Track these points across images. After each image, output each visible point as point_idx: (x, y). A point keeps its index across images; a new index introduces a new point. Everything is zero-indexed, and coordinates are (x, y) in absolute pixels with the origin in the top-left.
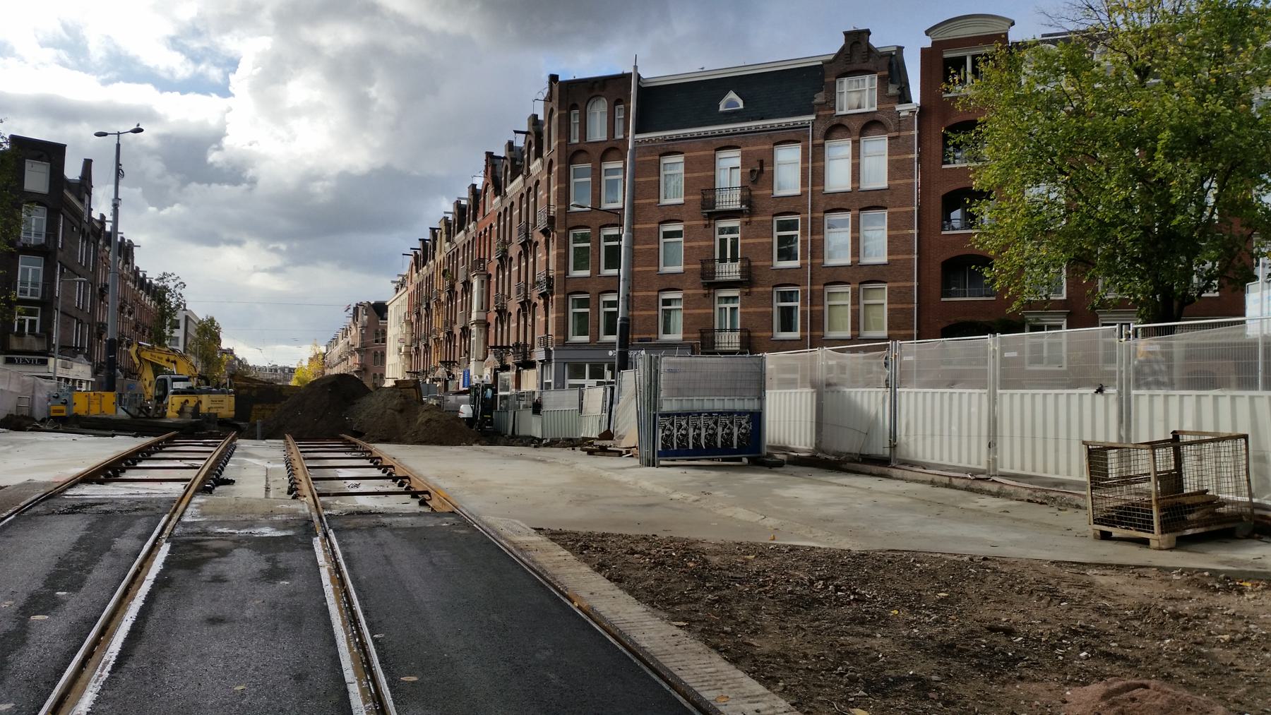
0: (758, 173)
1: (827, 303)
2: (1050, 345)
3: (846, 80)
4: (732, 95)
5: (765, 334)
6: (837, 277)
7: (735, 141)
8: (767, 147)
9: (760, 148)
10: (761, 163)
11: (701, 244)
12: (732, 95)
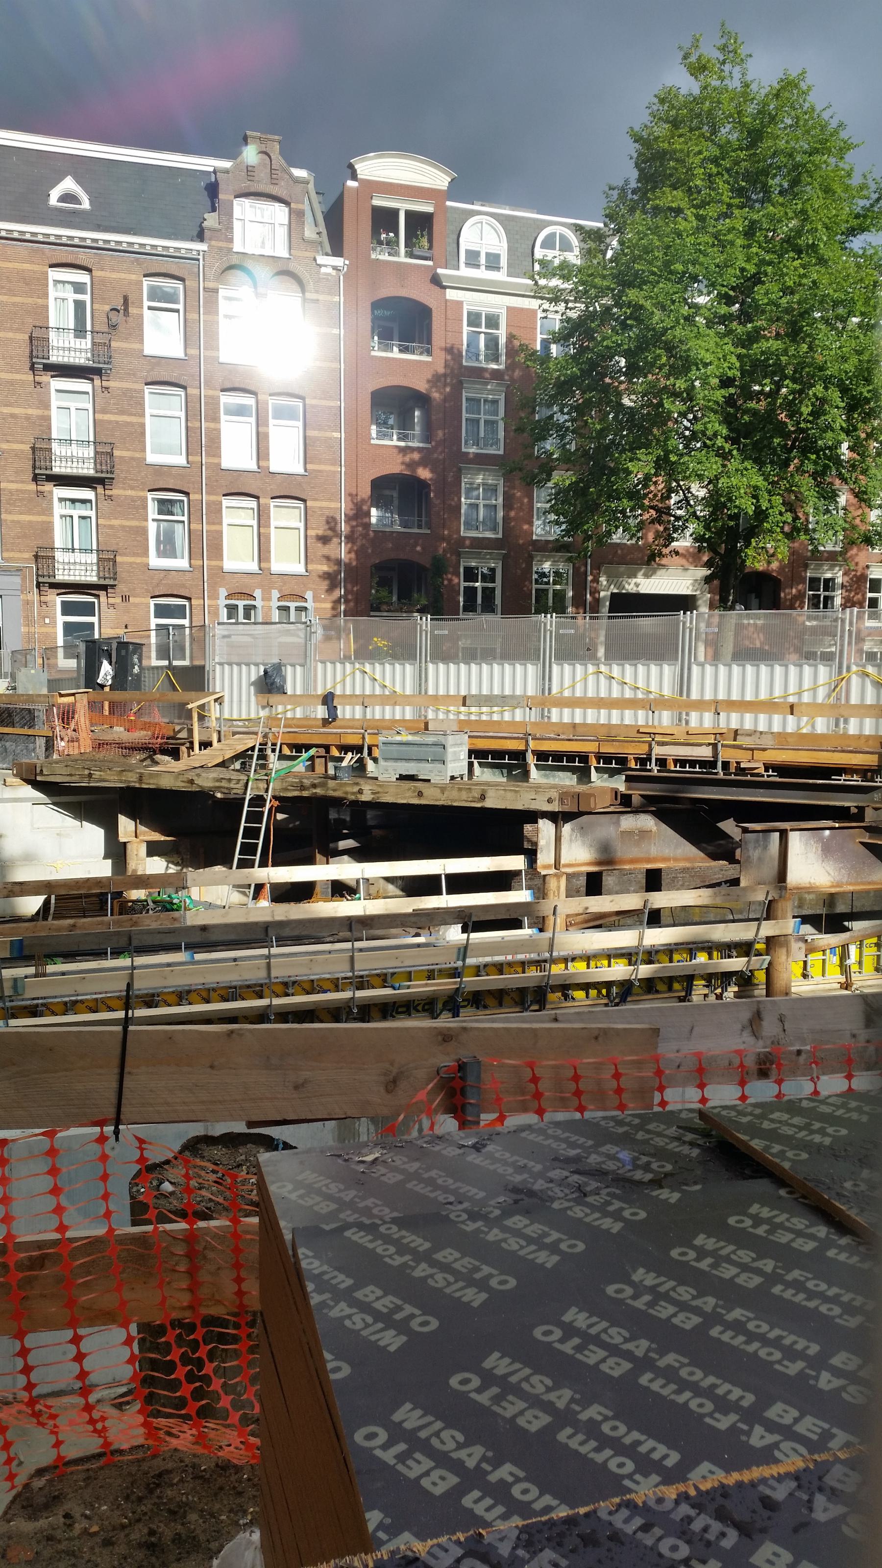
0: (117, 317)
1: (226, 520)
2: (484, 589)
3: (246, 202)
4: (68, 184)
5: (139, 560)
6: (238, 487)
7: (82, 257)
9: (120, 275)
10: (126, 299)
11: (30, 411)
12: (68, 184)
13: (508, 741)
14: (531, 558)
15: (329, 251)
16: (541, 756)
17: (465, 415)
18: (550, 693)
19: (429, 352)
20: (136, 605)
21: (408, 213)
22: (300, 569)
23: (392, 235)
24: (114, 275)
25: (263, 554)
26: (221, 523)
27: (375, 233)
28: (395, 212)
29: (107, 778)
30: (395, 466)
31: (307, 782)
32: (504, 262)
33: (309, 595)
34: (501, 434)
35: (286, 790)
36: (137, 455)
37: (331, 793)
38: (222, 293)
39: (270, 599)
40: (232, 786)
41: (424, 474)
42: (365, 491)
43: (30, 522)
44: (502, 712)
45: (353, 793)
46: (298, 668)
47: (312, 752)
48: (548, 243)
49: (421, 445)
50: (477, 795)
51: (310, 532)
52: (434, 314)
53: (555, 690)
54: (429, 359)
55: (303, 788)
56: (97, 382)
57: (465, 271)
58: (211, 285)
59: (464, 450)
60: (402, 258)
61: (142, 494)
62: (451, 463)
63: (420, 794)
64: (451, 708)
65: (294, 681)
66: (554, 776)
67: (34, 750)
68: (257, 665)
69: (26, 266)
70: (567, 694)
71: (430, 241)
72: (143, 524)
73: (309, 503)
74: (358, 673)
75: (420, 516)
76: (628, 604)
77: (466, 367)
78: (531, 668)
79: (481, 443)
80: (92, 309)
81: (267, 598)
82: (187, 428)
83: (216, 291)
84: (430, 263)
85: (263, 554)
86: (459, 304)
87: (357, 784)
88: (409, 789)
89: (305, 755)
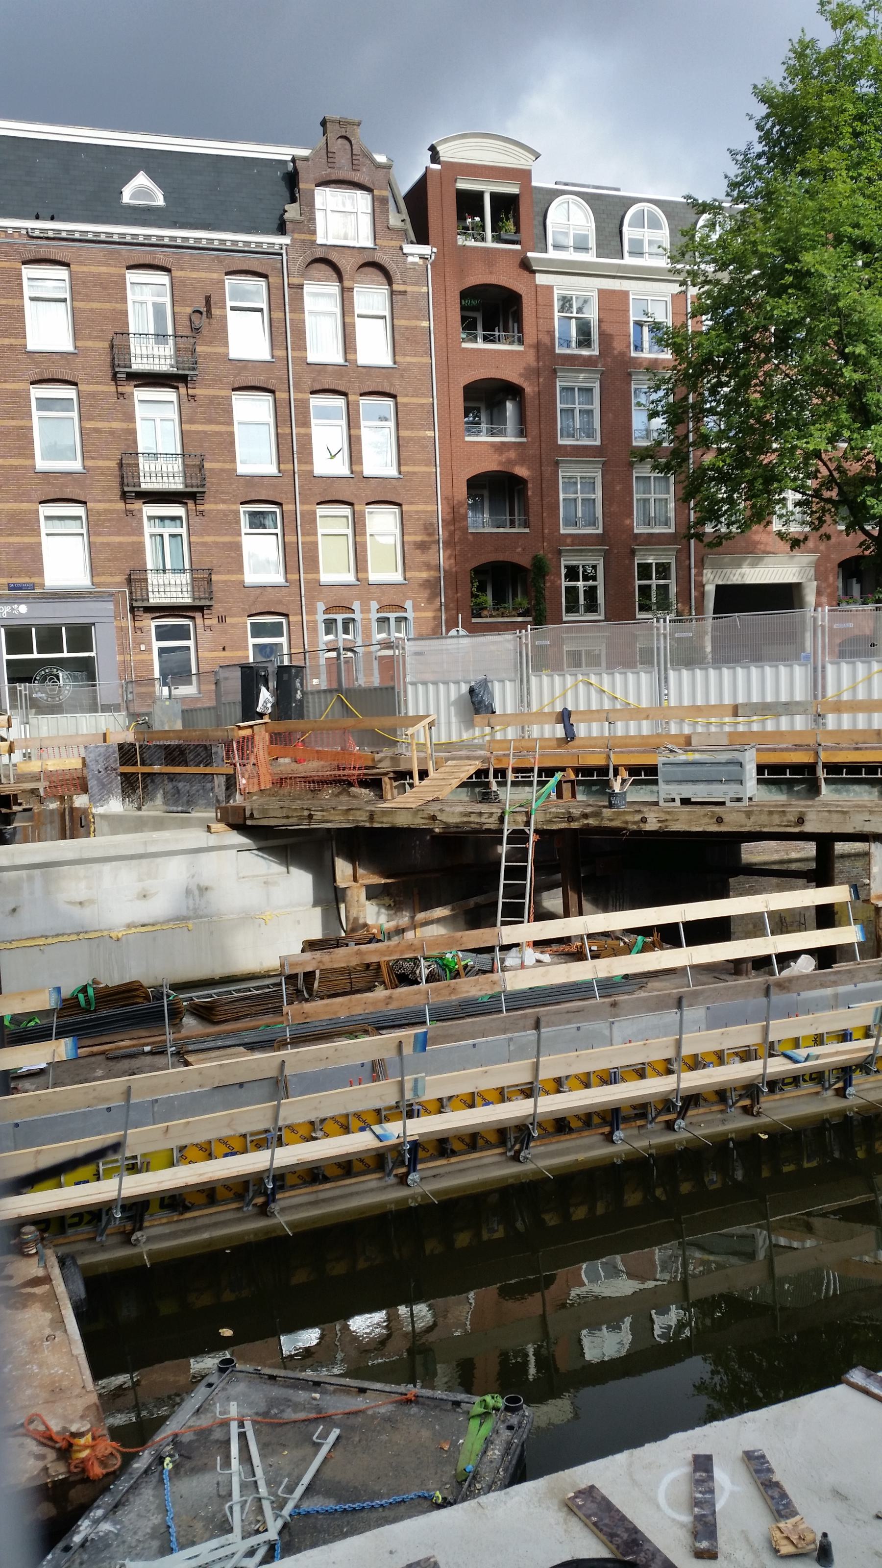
0: (200, 319)
1: (320, 531)
4: (141, 180)
5: (234, 577)
6: (332, 494)
7: (160, 257)
8: (215, 276)
9: (199, 275)
10: (208, 299)
11: (115, 425)
12: (141, 180)
13: (792, 754)
14: (633, 552)
15: (414, 240)
16: (833, 768)
17: (559, 406)
18: (824, 696)
19: (520, 341)
20: (233, 625)
21: (494, 196)
22: (397, 577)
23: (477, 219)
24: (195, 275)
25: (360, 563)
26: (316, 534)
27: (461, 218)
28: (480, 195)
29: (331, 818)
30: (491, 464)
31: (576, 812)
32: (592, 243)
33: (408, 605)
34: (597, 425)
35: (550, 821)
36: (227, 466)
37: (607, 823)
38: (306, 289)
39: (368, 611)
40: (483, 820)
41: (521, 471)
42: (462, 491)
43: (120, 543)
44: (763, 721)
45: (635, 823)
46: (508, 683)
47: (559, 776)
48: (638, 221)
49: (513, 440)
50: (792, 818)
51: (407, 538)
52: (524, 301)
53: (830, 692)
54: (521, 348)
55: (571, 818)
56: (183, 390)
57: (552, 254)
58: (295, 281)
59: (560, 442)
60: (489, 244)
61: (234, 507)
62: (550, 457)
63: (720, 820)
64: (713, 720)
65: (504, 698)
66: (848, 791)
67: (212, 789)
68: (457, 683)
69: (103, 269)
70: (845, 697)
71: (517, 224)
72: (237, 539)
73: (405, 508)
74: (581, 686)
75: (512, 513)
76: (735, 599)
77: (560, 355)
78: (798, 670)
79: (577, 435)
80: (174, 314)
81: (366, 610)
82: (277, 434)
83: (301, 287)
84: (518, 247)
85: (360, 563)
86: (550, 288)
87: (639, 812)
88: (705, 815)
89: (553, 781)
